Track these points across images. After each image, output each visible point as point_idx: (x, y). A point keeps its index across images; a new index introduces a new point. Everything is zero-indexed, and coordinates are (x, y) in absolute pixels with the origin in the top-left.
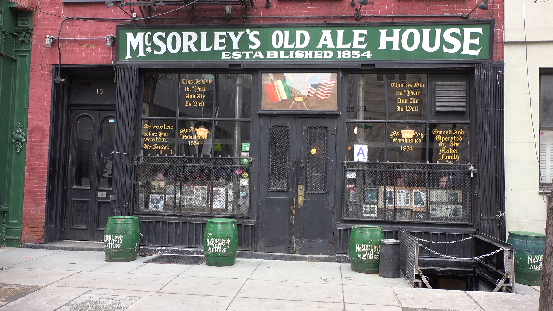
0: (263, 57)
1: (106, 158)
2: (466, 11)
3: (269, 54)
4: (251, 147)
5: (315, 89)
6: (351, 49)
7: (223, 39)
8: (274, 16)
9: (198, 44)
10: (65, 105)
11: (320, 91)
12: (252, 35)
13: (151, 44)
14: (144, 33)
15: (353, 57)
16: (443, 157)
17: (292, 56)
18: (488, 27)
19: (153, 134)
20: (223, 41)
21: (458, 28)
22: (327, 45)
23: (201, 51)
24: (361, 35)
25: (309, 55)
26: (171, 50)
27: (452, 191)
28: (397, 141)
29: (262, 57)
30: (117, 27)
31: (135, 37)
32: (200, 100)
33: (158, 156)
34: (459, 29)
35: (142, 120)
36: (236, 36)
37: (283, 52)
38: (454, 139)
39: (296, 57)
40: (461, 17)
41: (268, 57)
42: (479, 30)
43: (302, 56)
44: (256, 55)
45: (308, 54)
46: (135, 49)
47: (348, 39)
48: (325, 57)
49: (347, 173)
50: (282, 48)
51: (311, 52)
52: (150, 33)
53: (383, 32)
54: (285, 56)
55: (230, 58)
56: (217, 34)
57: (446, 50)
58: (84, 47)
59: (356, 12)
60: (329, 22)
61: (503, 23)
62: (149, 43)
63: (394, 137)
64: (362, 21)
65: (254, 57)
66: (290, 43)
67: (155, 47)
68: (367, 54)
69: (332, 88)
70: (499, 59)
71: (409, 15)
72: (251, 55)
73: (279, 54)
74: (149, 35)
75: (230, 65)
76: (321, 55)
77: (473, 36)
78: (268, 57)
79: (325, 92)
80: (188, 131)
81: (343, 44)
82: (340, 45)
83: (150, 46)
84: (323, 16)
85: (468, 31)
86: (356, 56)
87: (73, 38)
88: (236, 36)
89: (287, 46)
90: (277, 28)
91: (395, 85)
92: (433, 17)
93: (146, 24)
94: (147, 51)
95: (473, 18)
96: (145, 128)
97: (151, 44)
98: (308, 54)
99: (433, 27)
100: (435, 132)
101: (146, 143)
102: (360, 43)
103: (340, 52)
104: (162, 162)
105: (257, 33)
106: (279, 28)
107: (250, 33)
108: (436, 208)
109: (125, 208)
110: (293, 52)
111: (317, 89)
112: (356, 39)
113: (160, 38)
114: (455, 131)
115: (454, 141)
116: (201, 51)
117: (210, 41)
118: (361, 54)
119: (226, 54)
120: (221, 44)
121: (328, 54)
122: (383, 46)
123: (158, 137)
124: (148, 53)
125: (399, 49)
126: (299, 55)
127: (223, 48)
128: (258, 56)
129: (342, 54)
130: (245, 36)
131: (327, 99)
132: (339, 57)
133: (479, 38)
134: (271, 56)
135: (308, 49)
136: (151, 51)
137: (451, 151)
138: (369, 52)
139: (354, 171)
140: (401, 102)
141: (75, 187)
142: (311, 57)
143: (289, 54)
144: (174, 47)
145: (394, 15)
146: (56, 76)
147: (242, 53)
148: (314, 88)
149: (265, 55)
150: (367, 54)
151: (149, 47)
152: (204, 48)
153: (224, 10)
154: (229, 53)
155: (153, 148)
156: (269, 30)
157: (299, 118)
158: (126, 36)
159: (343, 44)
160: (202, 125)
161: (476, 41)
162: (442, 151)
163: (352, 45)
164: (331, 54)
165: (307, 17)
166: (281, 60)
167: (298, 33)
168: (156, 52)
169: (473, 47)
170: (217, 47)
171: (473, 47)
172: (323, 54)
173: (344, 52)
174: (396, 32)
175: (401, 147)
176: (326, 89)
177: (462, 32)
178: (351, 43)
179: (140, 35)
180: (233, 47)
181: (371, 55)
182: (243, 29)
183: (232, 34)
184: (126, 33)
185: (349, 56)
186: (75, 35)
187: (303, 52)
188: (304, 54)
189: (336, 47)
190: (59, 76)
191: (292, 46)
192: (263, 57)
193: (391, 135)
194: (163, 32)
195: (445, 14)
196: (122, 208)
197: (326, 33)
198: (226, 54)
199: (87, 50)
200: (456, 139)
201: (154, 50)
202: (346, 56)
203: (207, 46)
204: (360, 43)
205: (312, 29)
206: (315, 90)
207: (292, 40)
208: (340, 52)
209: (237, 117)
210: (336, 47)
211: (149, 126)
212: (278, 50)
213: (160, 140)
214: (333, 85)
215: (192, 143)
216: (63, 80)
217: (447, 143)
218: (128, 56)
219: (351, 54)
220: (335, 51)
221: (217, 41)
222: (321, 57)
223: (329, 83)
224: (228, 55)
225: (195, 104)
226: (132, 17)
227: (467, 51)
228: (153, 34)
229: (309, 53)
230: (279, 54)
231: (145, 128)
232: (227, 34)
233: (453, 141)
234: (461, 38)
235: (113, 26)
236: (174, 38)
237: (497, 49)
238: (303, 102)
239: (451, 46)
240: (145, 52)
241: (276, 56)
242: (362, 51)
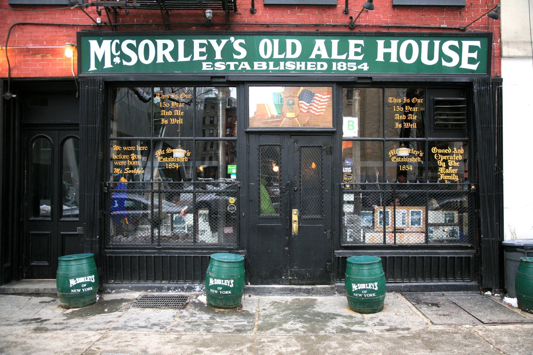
0: (250, 69)
1: (69, 184)
2: (463, 23)
3: (256, 65)
4: (238, 169)
5: (308, 103)
6: (347, 61)
7: (203, 47)
8: (260, 23)
9: (174, 53)
10: (17, 124)
11: (313, 106)
12: (237, 43)
13: (119, 53)
14: (111, 41)
15: (349, 69)
16: (441, 177)
17: (282, 68)
18: (486, 40)
19: (124, 157)
20: (204, 50)
21: (456, 40)
22: (320, 55)
23: (178, 61)
24: (357, 46)
25: (301, 66)
27: (448, 211)
28: (395, 160)
29: (248, 68)
30: (78, 33)
31: (100, 45)
32: (177, 117)
33: (132, 182)
34: (457, 42)
35: (110, 140)
36: (219, 45)
37: (273, 63)
38: (453, 157)
39: (286, 68)
40: (458, 29)
41: (256, 68)
42: (477, 43)
43: (293, 67)
44: (241, 67)
45: (301, 66)
46: (100, 59)
47: (343, 49)
48: (319, 68)
49: (344, 196)
50: (271, 59)
51: (303, 63)
52: (118, 41)
53: (381, 43)
54: (274, 67)
55: (212, 69)
56: (197, 43)
57: (444, 63)
58: (39, 57)
59: (350, 20)
60: (322, 30)
61: (499, 36)
62: (117, 52)
63: (392, 156)
64: (357, 30)
65: (240, 69)
66: (280, 53)
67: (125, 57)
68: (363, 66)
69: (326, 103)
70: (496, 74)
71: (405, 25)
72: (236, 66)
73: (268, 65)
74: (117, 43)
75: (212, 77)
76: (314, 66)
77: (472, 49)
78: (256, 68)
79: (319, 107)
80: (165, 152)
81: (339, 54)
83: (118, 56)
84: (315, 23)
85: (466, 44)
86: (352, 68)
87: (24, 46)
88: (219, 45)
89: (276, 56)
90: (265, 36)
91: (393, 99)
92: (429, 28)
93: (113, 30)
94: (114, 61)
95: (470, 31)
96: (114, 149)
97: (119, 53)
98: (301, 66)
99: (432, 38)
100: (434, 150)
101: (118, 167)
102: (356, 54)
103: (335, 63)
104: (136, 189)
105: (243, 41)
106: (267, 36)
107: (235, 40)
108: (433, 230)
109: (96, 242)
110: (283, 63)
111: (311, 104)
112: (352, 49)
113: (130, 46)
114: (455, 149)
115: (453, 160)
116: (178, 61)
117: (189, 51)
118: (357, 66)
119: (207, 65)
120: (202, 54)
121: (322, 66)
122: (380, 58)
123: (131, 160)
124: (116, 63)
125: (397, 62)
126: (290, 66)
127: (204, 58)
128: (244, 67)
129: (337, 66)
130: (229, 45)
131: (321, 115)
132: (334, 68)
133: (477, 52)
134: (259, 67)
135: (300, 59)
136: (120, 61)
138: (365, 64)
139: (352, 193)
140: (399, 118)
141: (32, 218)
142: (303, 68)
143: (279, 65)
144: (147, 57)
145: (390, 25)
146: (5, 91)
147: (226, 63)
148: (308, 103)
149: (252, 66)
150: (363, 66)
151: (117, 57)
152: (181, 58)
153: (205, 16)
154: (211, 63)
155: (125, 172)
156: (256, 37)
157: (291, 136)
158: (89, 44)
159: (339, 54)
160: (179, 146)
161: (475, 55)
162: (441, 170)
163: (348, 56)
164: (326, 66)
165: (297, 25)
166: (271, 72)
167: (289, 42)
168: (125, 63)
169: (471, 61)
170: (197, 57)
171: (471, 61)
172: (316, 66)
173: (339, 64)
174: (394, 43)
175: (400, 166)
176: (320, 104)
177: (461, 44)
178: (346, 55)
179: (106, 43)
180: (215, 57)
181: (368, 68)
182: (226, 36)
183: (213, 42)
184: (90, 41)
185: (345, 68)
186: (27, 43)
187: (294, 63)
188: (296, 65)
189: (331, 58)
190: (9, 91)
191: (282, 56)
192: (250, 69)
193: (390, 154)
194: (133, 40)
195: (442, 26)
196: (92, 242)
197: (320, 43)
198: (207, 65)
199: (43, 60)
200: (455, 158)
201: (123, 61)
202: (342, 68)
203: (186, 56)
204: (356, 54)
205: (303, 37)
206: (308, 105)
207: (282, 49)
208: (335, 63)
209: (221, 135)
210: (331, 58)
211: (119, 148)
212: (267, 61)
213: (132, 163)
214: (328, 99)
215: (170, 166)
216: (14, 96)
217: (446, 161)
218: (93, 67)
219: (347, 66)
220: (330, 62)
221: (197, 50)
222: (315, 69)
223: (323, 97)
224: (210, 66)
225: (172, 122)
226: (96, 22)
227: (465, 65)
228: (121, 42)
229: (301, 64)
230: (268, 65)
231: (114, 149)
232: (209, 42)
233: (452, 160)
234: (459, 51)
235: (73, 33)
236: (147, 46)
237: (494, 64)
238: (296, 118)
239: (449, 59)
240: (112, 63)
241: (264, 67)
242: (358, 63)
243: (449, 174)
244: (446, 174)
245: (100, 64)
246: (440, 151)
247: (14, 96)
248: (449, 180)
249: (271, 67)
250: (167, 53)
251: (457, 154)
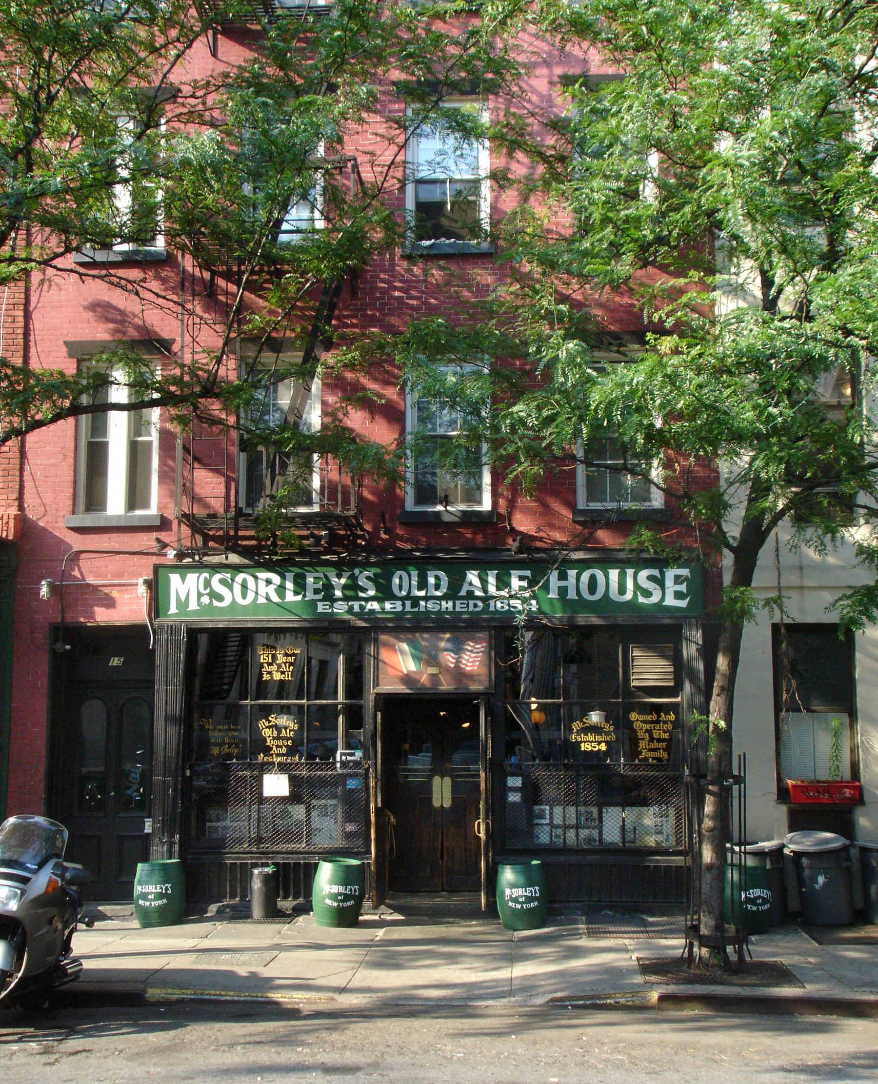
17: (422, 609)
22: (473, 592)
25: (447, 605)
26: (239, 600)
31: (183, 581)
43: (437, 608)
46: (183, 599)
47: (503, 583)
48: (471, 609)
50: (408, 597)
51: (450, 603)
52: (207, 575)
62: (205, 589)
67: (215, 596)
81: (498, 588)
82: (492, 589)
97: (208, 590)
112: (516, 583)
113: (223, 582)
121: (475, 606)
127: (320, 597)
132: (492, 609)
135: (445, 597)
137: (654, 745)
142: (451, 609)
144: (244, 596)
146: (55, 640)
162: (642, 744)
172: (468, 605)
179: (192, 577)
185: (507, 608)
207: (422, 585)
212: (403, 599)
216: (68, 647)
218: (173, 610)
228: (211, 577)
230: (404, 605)
234: (660, 582)
240: (199, 603)
241: (399, 608)
243: (655, 750)
244: (651, 750)
245: (183, 605)
246: (642, 718)
247: (68, 647)
248: (654, 759)
249: (408, 608)
250: (271, 590)
251: (665, 722)
